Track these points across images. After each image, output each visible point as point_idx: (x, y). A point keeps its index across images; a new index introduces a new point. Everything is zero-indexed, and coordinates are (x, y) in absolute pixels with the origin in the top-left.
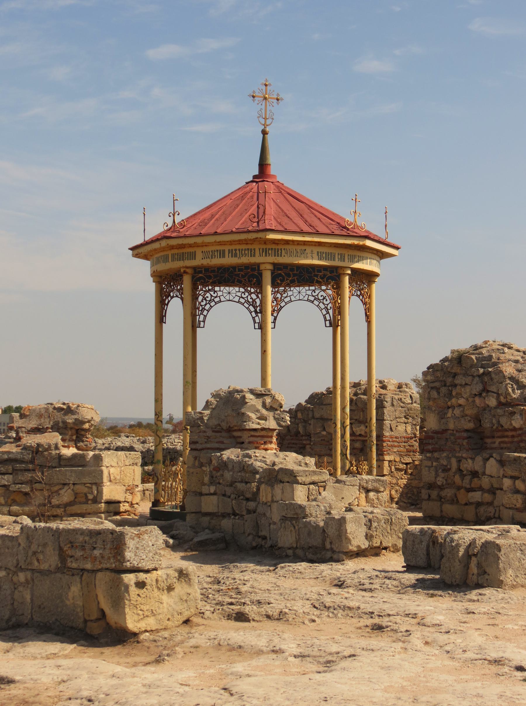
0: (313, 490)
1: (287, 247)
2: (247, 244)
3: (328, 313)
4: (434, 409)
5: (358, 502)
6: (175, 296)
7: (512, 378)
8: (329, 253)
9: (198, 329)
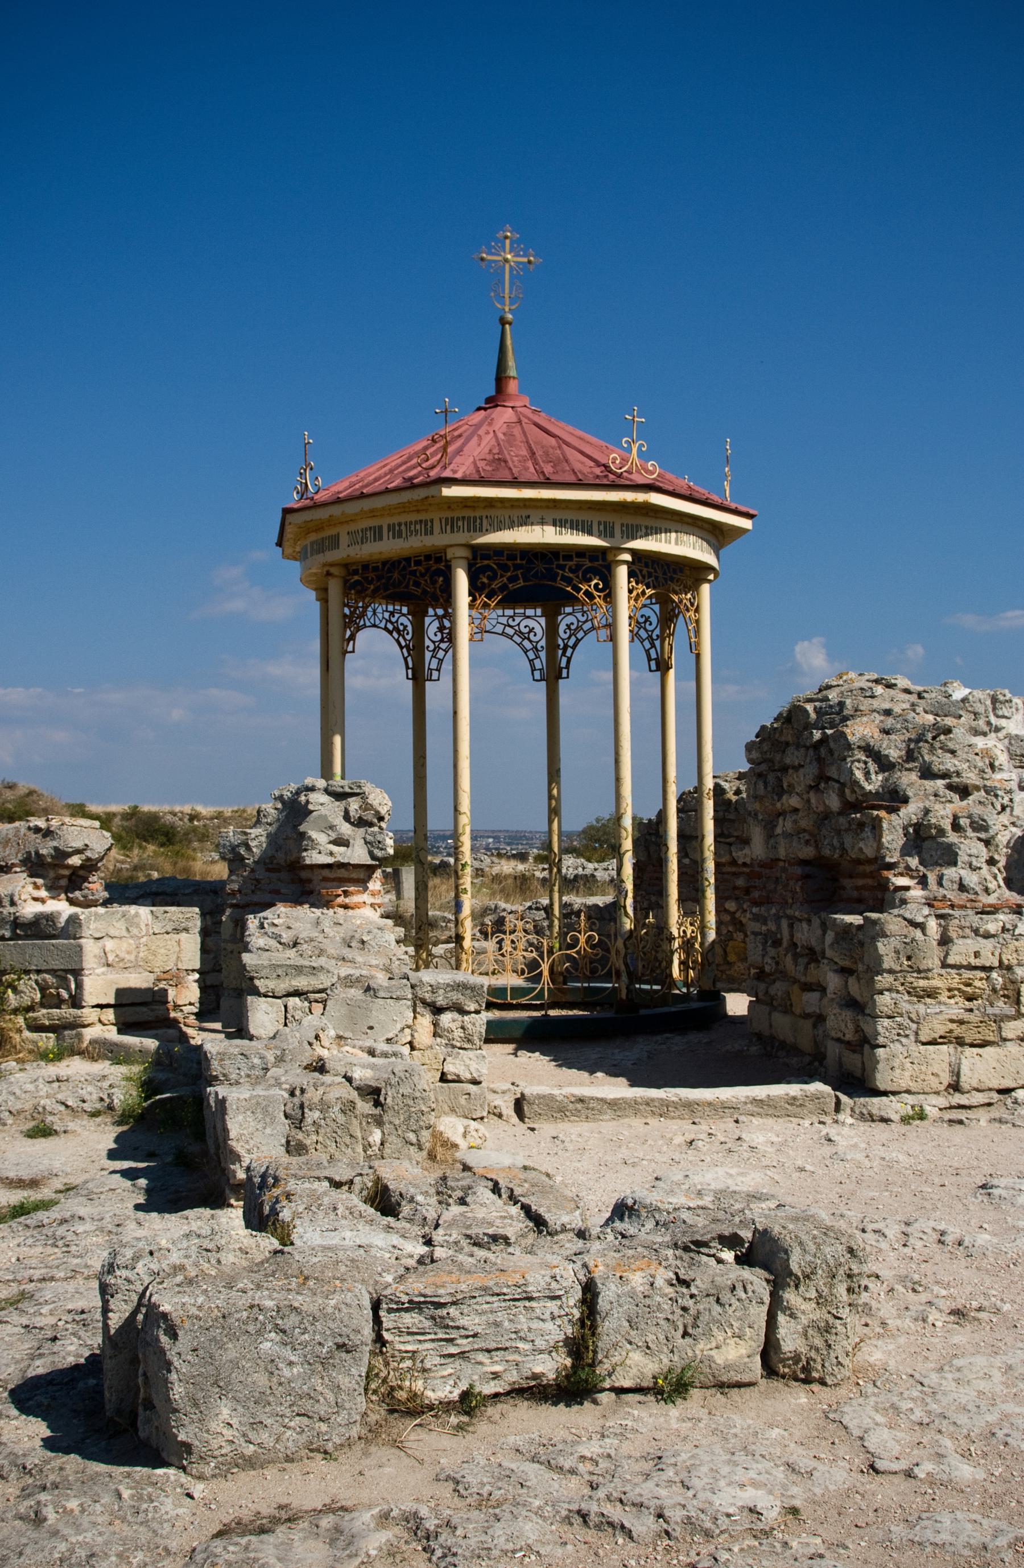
0: (295, 1009)
1: (492, 512)
2: (418, 511)
3: (653, 646)
4: (760, 817)
5: (412, 1036)
6: (368, 624)
7: (868, 750)
8: (578, 521)
9: (428, 684)
